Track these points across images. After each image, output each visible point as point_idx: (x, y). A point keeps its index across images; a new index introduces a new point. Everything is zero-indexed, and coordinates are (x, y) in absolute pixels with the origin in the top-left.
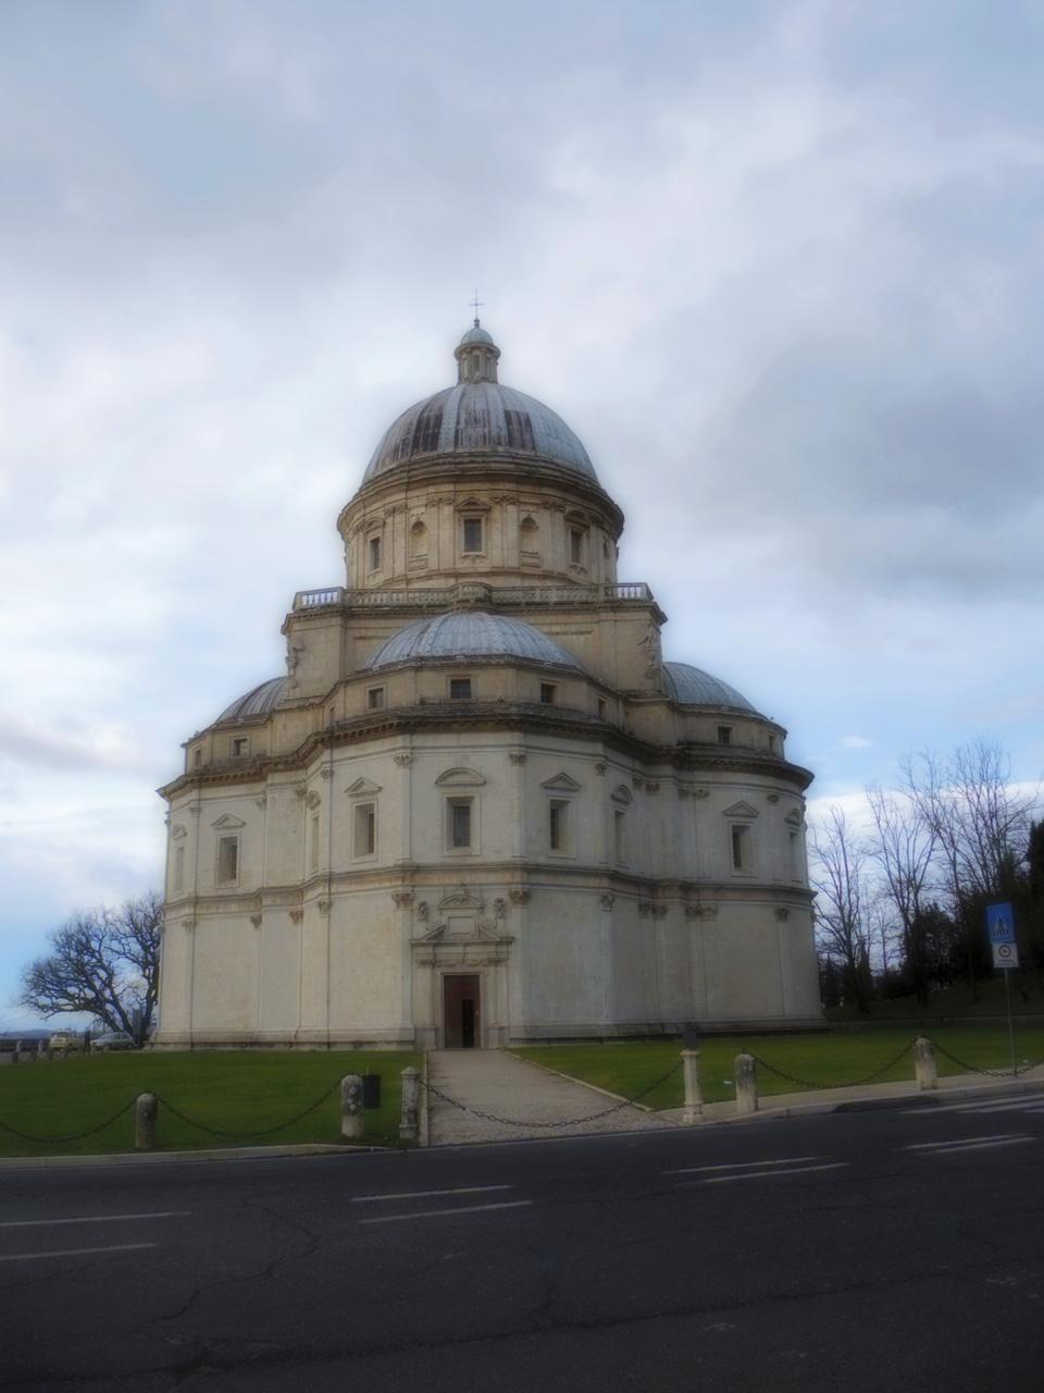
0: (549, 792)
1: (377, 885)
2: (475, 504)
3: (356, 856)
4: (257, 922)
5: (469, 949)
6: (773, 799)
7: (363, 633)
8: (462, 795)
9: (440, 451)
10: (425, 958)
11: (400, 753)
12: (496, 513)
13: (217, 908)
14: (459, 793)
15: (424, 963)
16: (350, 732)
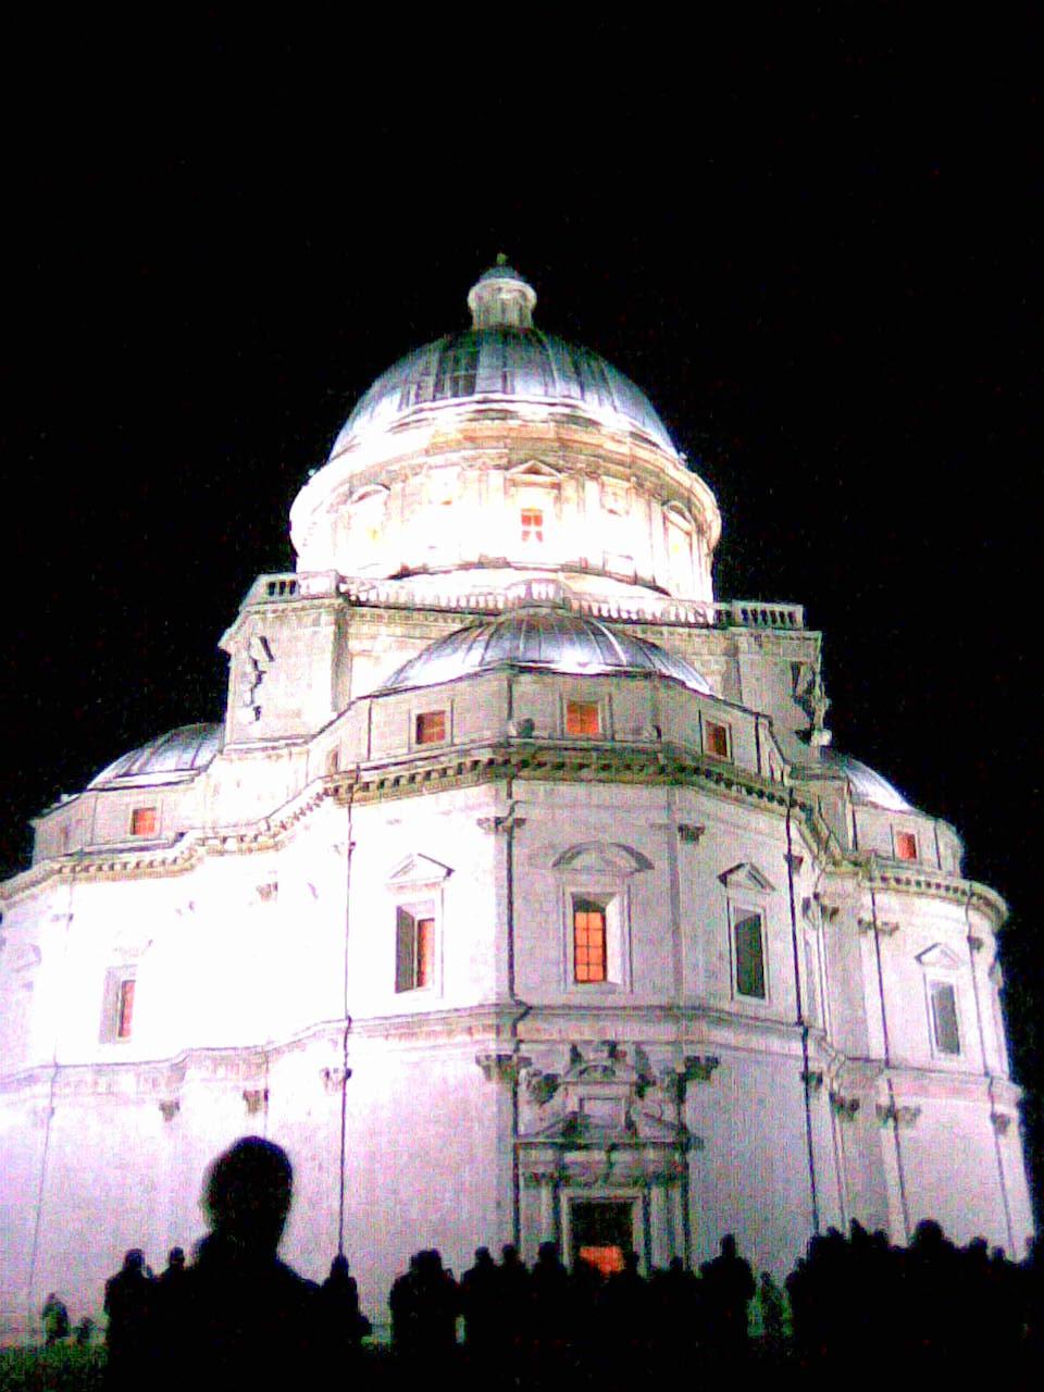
0: (731, 892)
1: (442, 1040)
2: (537, 472)
3: (399, 989)
4: (170, 1110)
5: (615, 1156)
6: (974, 943)
7: (367, 645)
8: (598, 890)
9: (478, 397)
10: (541, 1170)
11: (493, 812)
12: (569, 490)
13: (96, 1083)
14: (588, 886)
15: (537, 1179)
16: (392, 777)
